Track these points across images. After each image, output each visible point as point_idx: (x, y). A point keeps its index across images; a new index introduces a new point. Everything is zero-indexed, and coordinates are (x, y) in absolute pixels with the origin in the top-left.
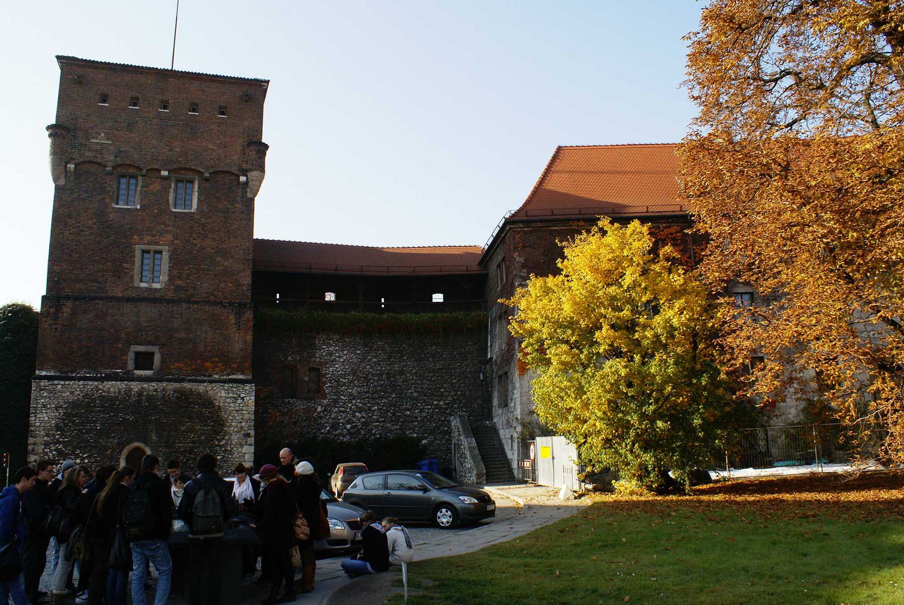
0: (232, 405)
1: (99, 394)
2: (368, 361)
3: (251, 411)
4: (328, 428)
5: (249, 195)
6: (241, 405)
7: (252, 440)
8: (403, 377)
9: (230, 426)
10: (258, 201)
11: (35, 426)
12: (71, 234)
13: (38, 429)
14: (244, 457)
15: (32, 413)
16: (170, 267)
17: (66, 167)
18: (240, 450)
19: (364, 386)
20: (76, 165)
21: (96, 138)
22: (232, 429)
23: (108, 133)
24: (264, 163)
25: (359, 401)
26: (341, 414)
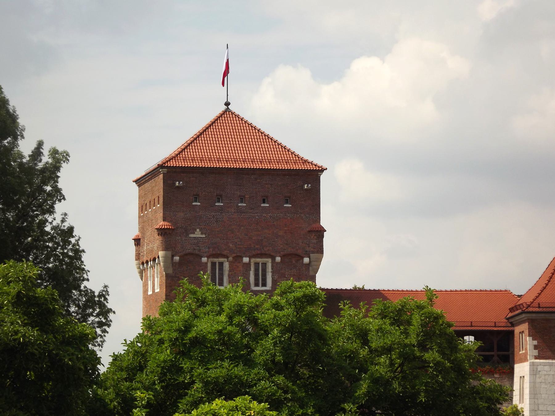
5: (311, 273)
17: (172, 259)
20: (180, 257)
21: (194, 233)
23: (202, 228)
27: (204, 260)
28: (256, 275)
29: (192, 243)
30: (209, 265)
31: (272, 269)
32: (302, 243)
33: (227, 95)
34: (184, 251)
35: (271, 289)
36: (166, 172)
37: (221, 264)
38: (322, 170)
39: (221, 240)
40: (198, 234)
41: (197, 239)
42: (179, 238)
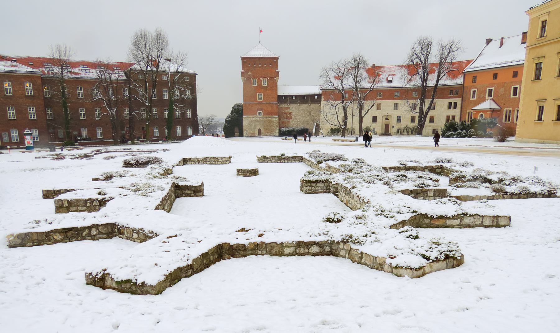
27: (251, 79)
30: (253, 80)
37: (256, 80)
40: (250, 73)
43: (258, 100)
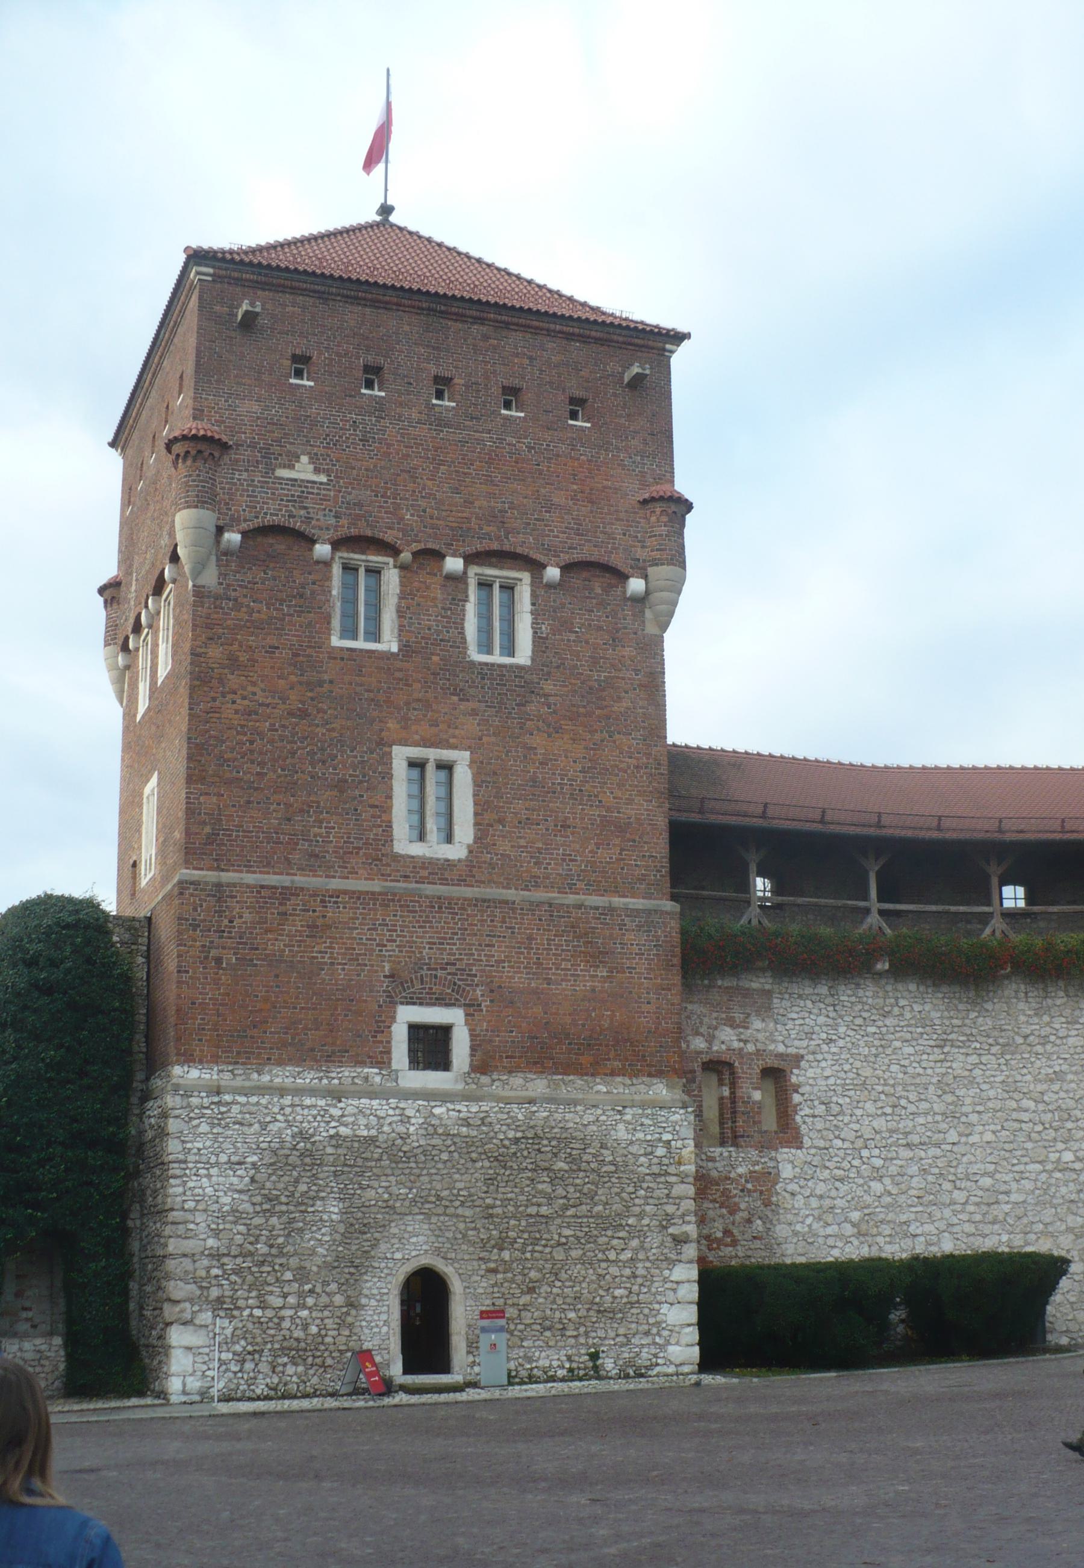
0: (642, 1159)
1: (332, 1132)
2: (894, 1053)
3: (687, 1176)
4: (809, 1221)
5: (651, 629)
6: (665, 1161)
7: (691, 1251)
8: (971, 1092)
9: (641, 1216)
10: (671, 639)
11: (183, 1209)
12: (237, 712)
13: (190, 1217)
14: (674, 1290)
15: (175, 1177)
16: (475, 804)
18: (666, 1273)
19: (885, 1114)
20: (245, 534)
21: (291, 467)
22: (646, 1221)
23: (316, 454)
24: (682, 547)
25: (876, 1152)
26: (837, 1184)
27: (322, 550)
28: (486, 617)
29: (287, 495)
31: (533, 604)
32: (624, 535)
33: (386, 190)
34: (257, 517)
35: (529, 663)
36: (210, 278)
38: (679, 338)
39: (376, 496)
40: (304, 470)
41: (300, 486)
42: (245, 475)
43: (404, 844)
